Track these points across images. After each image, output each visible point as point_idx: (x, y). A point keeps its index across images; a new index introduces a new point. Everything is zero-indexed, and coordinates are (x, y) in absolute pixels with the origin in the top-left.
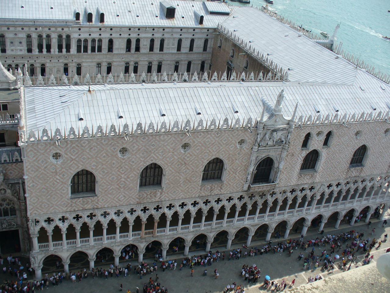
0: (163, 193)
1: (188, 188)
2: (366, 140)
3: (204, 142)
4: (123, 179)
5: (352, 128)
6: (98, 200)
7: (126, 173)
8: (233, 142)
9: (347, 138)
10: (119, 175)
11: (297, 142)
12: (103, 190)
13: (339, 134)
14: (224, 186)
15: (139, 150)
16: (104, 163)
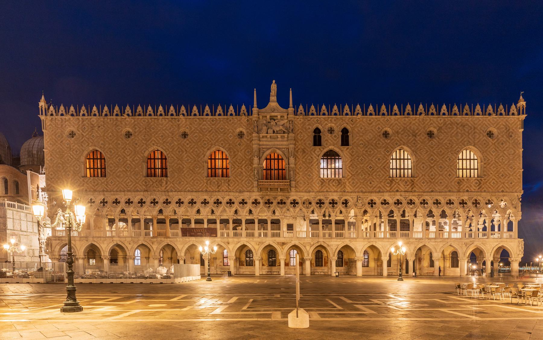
0: (169, 183)
1: (193, 179)
2: (401, 140)
3: (201, 128)
4: (128, 162)
5: (374, 124)
6: (107, 182)
7: (131, 156)
8: (230, 130)
9: (372, 136)
10: (124, 157)
11: (304, 136)
12: (111, 171)
13: (359, 131)
14: (231, 183)
15: (140, 132)
16: (111, 142)
